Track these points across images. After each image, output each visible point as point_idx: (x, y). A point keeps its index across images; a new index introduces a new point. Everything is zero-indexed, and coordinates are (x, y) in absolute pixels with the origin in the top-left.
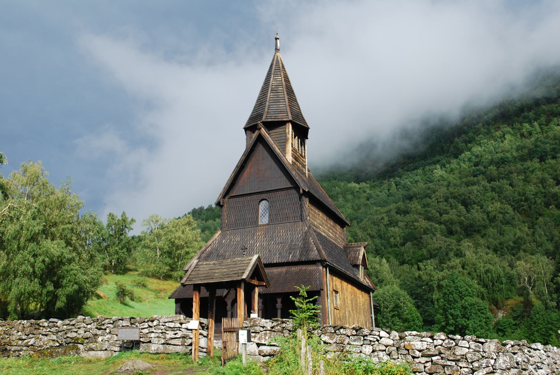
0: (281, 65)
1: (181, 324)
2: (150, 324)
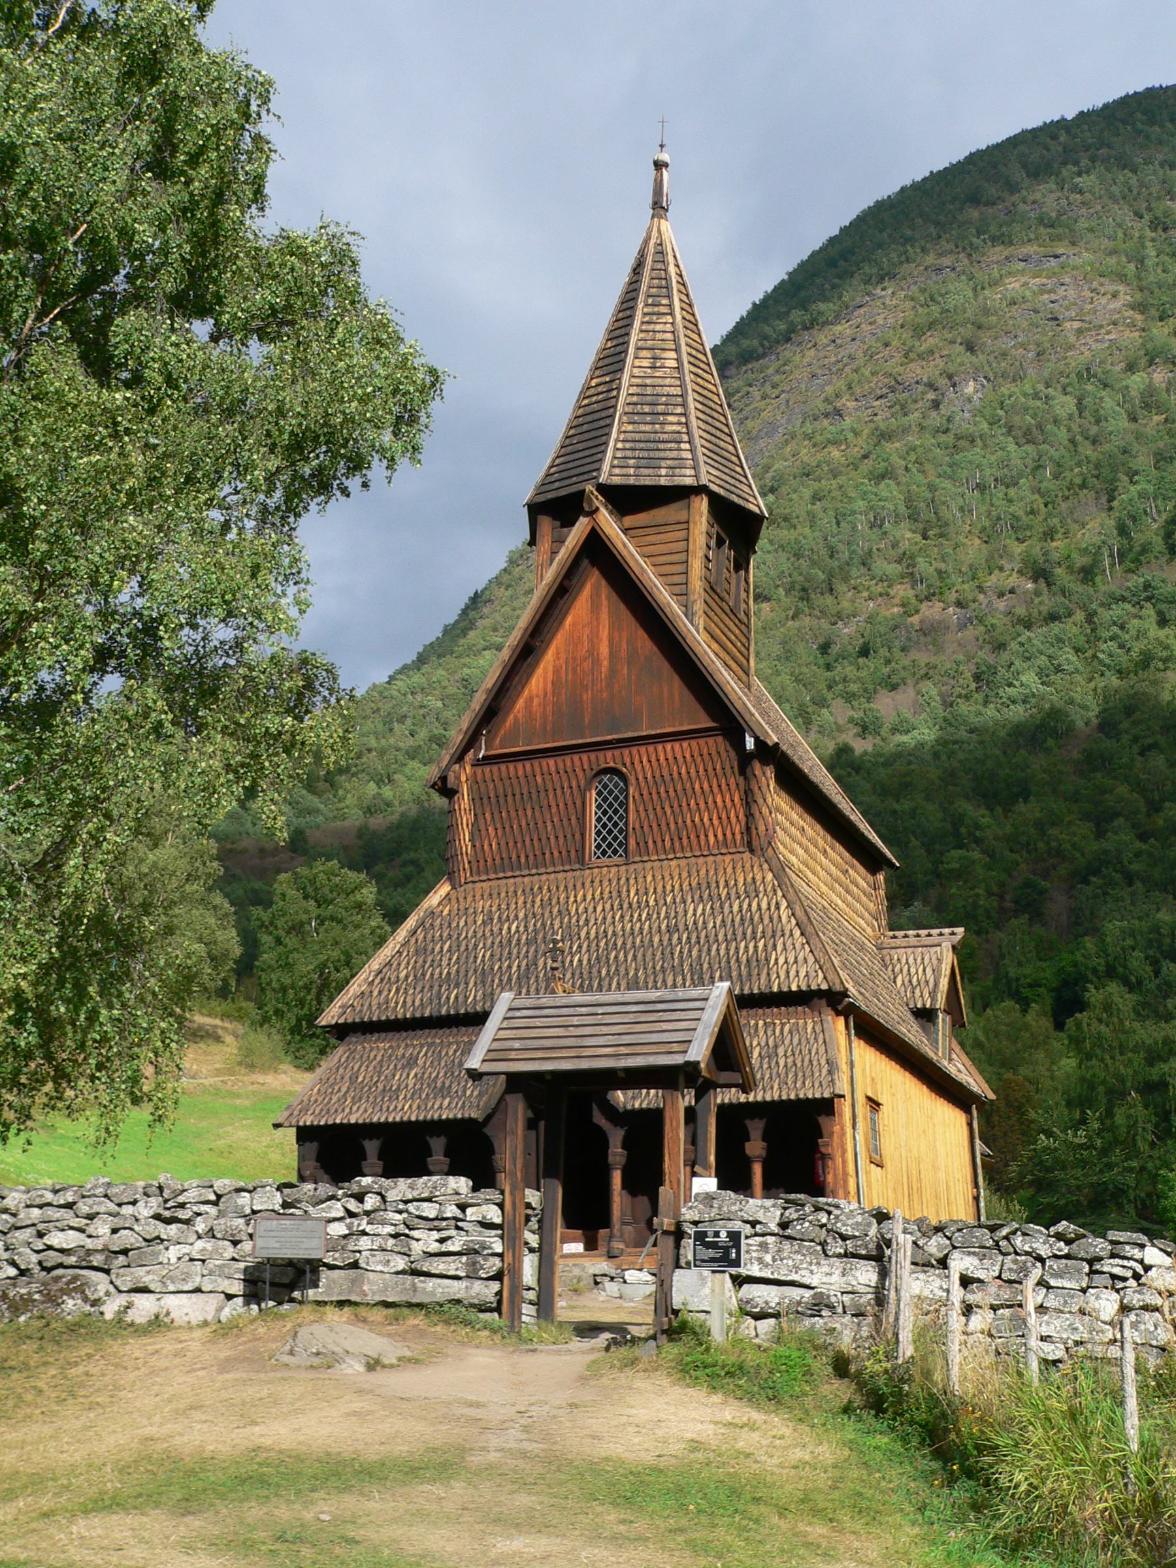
0: (672, 269)
1: (463, 1207)
2: (353, 1205)
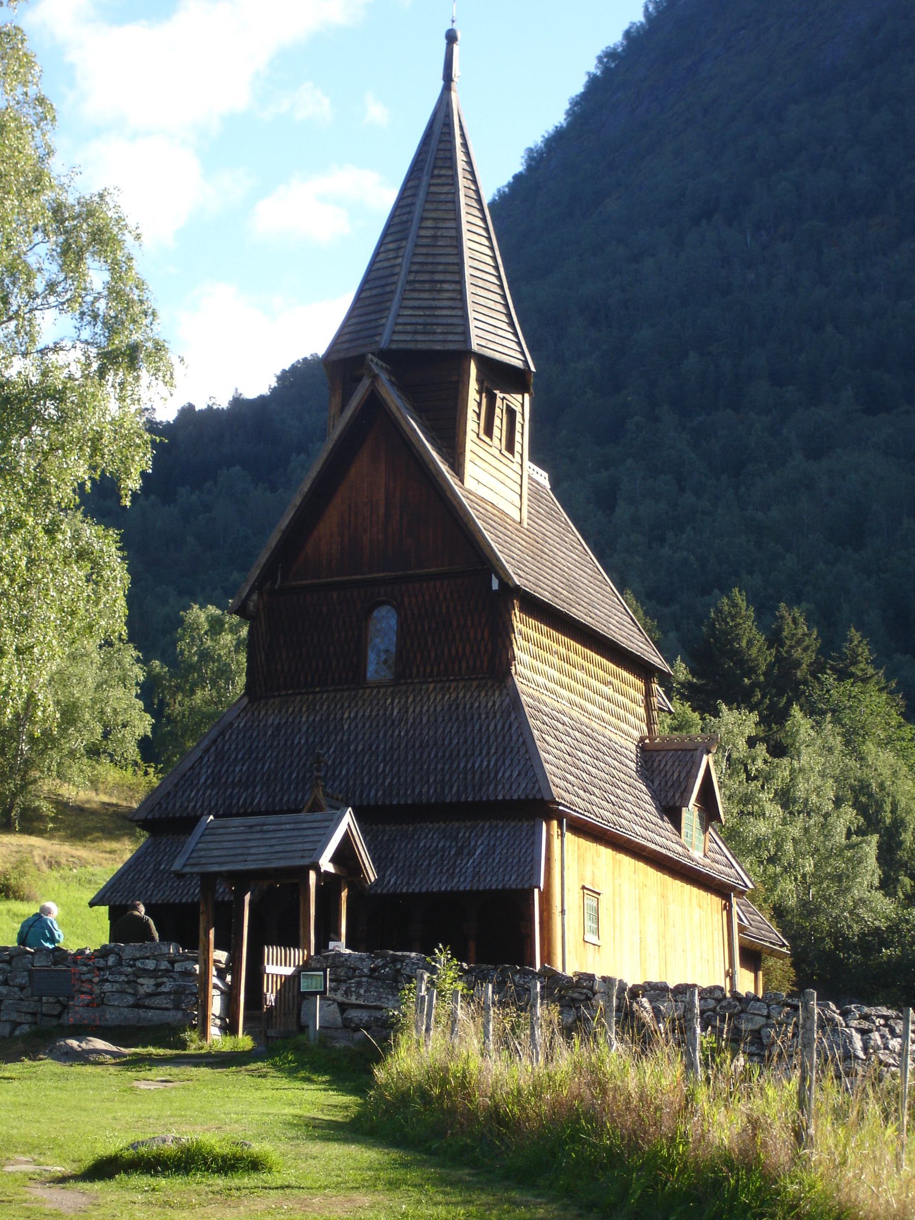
1: (172, 962)
2: (102, 963)
